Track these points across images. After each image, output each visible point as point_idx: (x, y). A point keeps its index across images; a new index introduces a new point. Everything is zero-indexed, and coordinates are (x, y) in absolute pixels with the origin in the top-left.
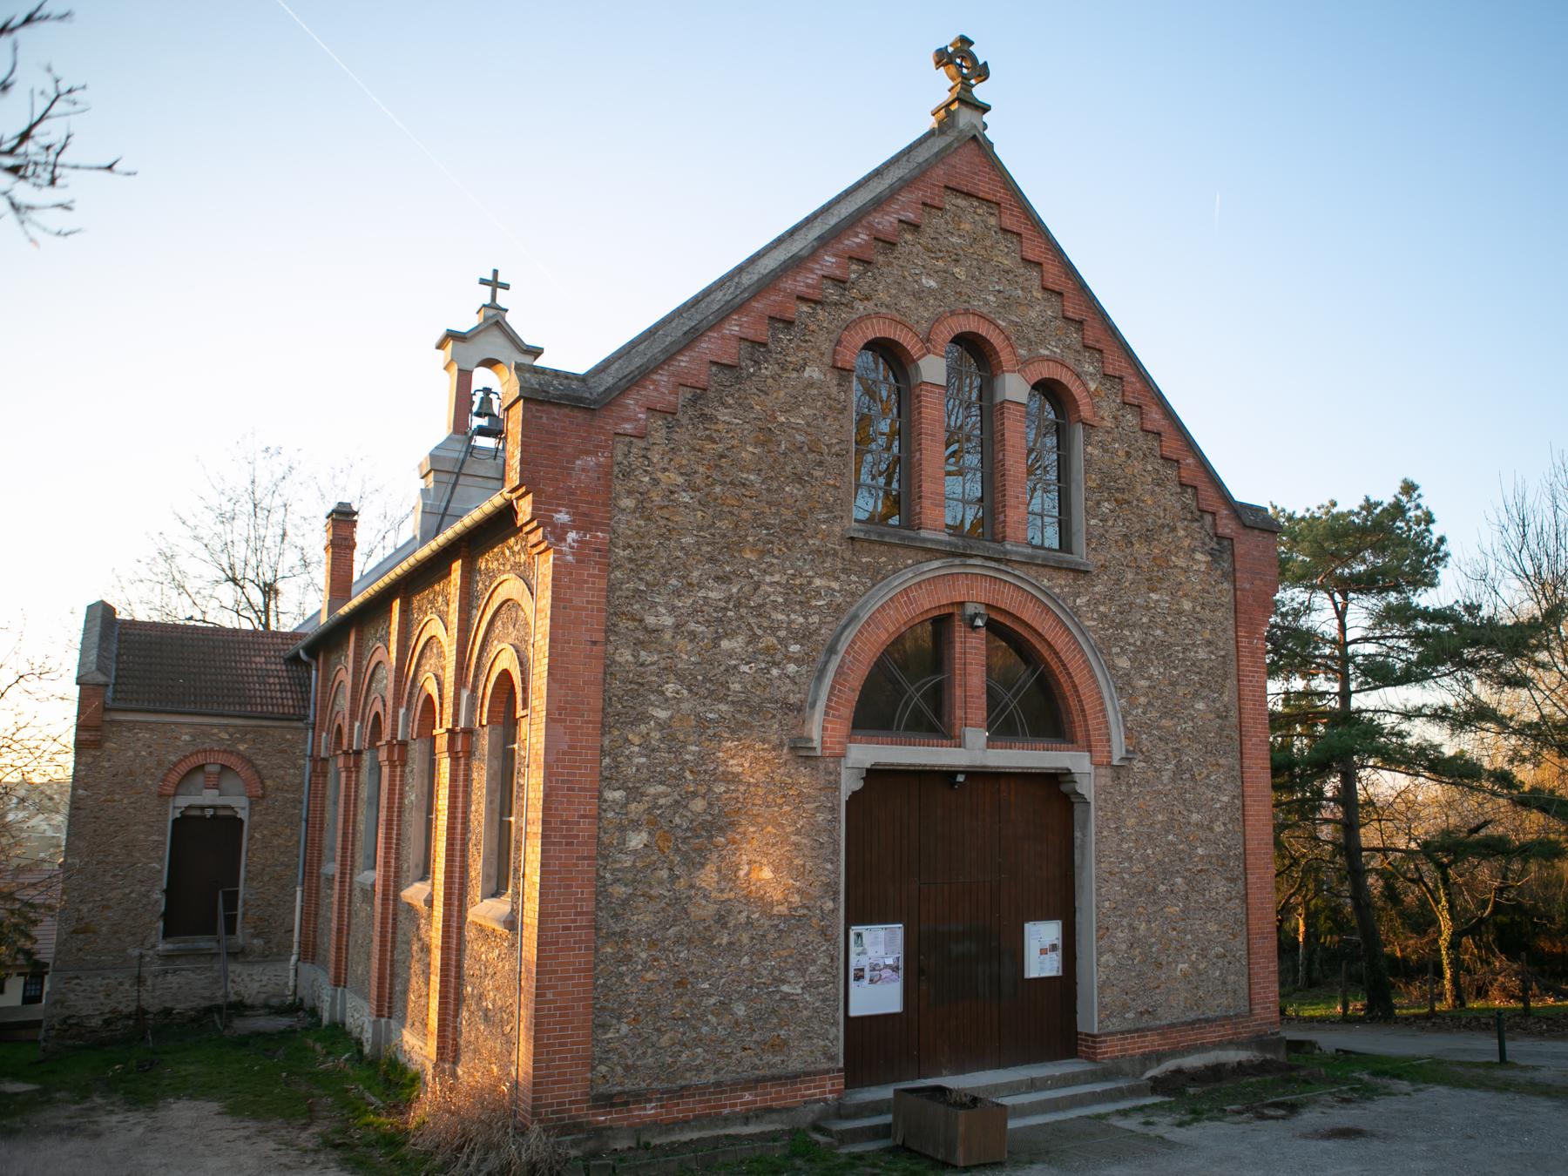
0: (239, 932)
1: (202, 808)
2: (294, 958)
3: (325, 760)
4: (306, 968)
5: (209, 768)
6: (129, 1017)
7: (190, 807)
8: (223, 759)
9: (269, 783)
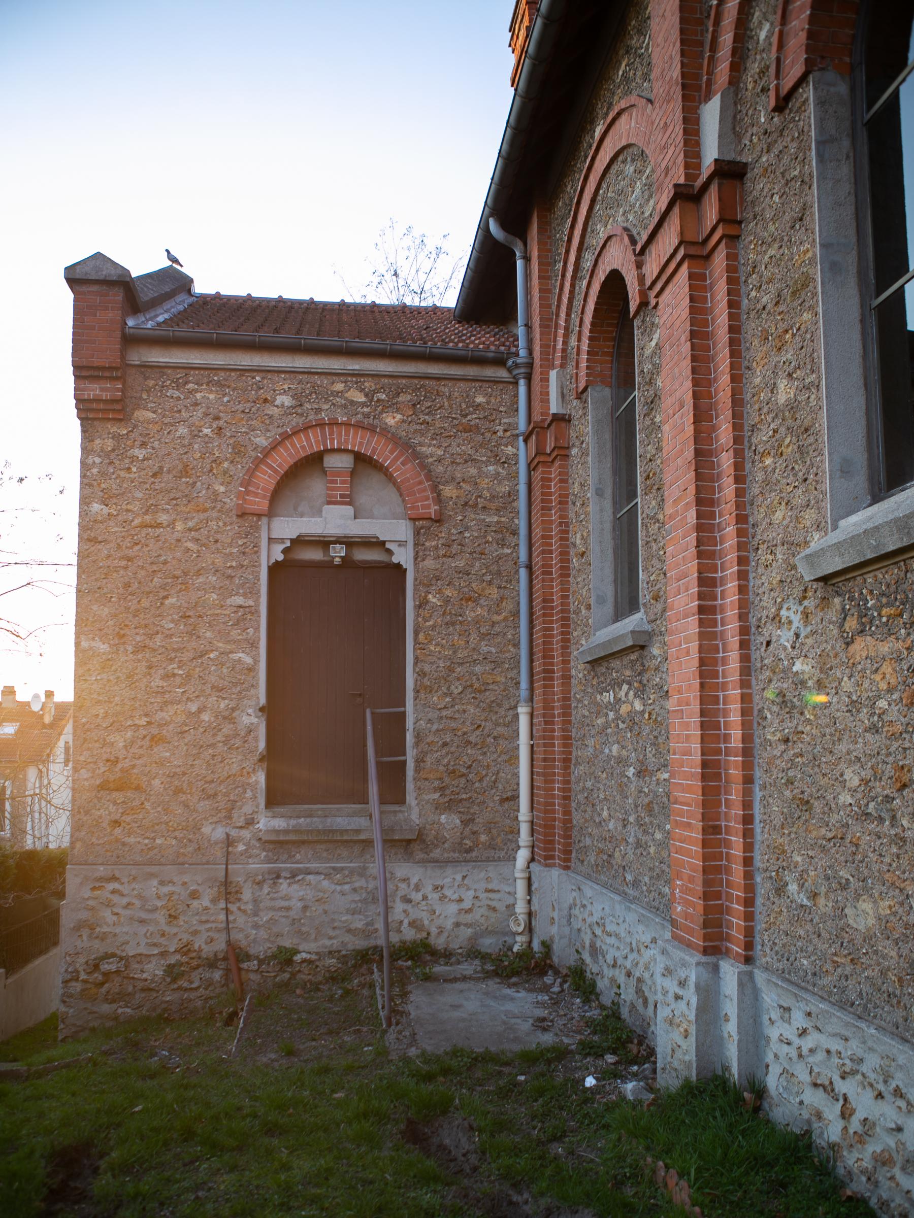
0: (411, 798)
1: (324, 543)
2: (523, 855)
3: (560, 419)
4: (551, 878)
5: (331, 461)
6: (212, 964)
7: (299, 542)
8: (357, 441)
9: (448, 491)
